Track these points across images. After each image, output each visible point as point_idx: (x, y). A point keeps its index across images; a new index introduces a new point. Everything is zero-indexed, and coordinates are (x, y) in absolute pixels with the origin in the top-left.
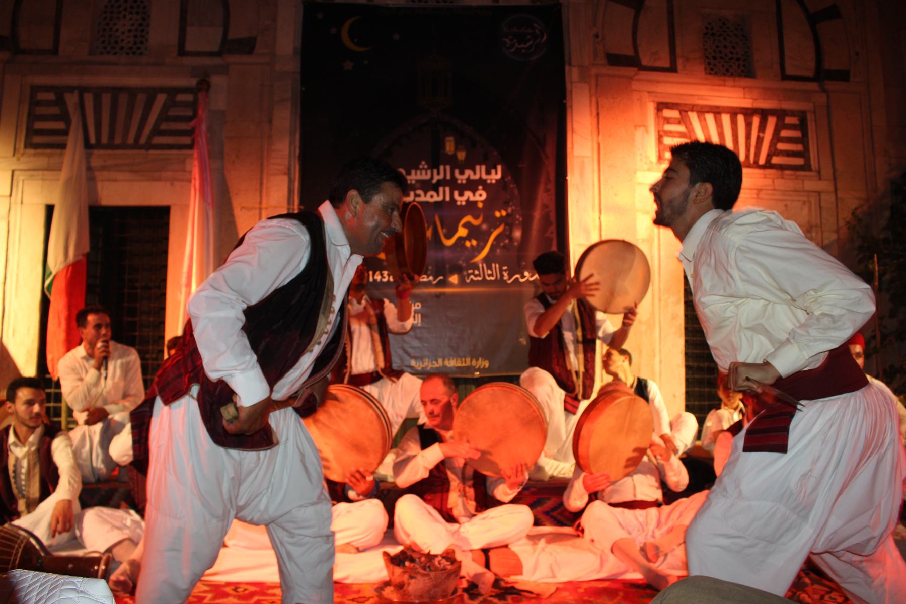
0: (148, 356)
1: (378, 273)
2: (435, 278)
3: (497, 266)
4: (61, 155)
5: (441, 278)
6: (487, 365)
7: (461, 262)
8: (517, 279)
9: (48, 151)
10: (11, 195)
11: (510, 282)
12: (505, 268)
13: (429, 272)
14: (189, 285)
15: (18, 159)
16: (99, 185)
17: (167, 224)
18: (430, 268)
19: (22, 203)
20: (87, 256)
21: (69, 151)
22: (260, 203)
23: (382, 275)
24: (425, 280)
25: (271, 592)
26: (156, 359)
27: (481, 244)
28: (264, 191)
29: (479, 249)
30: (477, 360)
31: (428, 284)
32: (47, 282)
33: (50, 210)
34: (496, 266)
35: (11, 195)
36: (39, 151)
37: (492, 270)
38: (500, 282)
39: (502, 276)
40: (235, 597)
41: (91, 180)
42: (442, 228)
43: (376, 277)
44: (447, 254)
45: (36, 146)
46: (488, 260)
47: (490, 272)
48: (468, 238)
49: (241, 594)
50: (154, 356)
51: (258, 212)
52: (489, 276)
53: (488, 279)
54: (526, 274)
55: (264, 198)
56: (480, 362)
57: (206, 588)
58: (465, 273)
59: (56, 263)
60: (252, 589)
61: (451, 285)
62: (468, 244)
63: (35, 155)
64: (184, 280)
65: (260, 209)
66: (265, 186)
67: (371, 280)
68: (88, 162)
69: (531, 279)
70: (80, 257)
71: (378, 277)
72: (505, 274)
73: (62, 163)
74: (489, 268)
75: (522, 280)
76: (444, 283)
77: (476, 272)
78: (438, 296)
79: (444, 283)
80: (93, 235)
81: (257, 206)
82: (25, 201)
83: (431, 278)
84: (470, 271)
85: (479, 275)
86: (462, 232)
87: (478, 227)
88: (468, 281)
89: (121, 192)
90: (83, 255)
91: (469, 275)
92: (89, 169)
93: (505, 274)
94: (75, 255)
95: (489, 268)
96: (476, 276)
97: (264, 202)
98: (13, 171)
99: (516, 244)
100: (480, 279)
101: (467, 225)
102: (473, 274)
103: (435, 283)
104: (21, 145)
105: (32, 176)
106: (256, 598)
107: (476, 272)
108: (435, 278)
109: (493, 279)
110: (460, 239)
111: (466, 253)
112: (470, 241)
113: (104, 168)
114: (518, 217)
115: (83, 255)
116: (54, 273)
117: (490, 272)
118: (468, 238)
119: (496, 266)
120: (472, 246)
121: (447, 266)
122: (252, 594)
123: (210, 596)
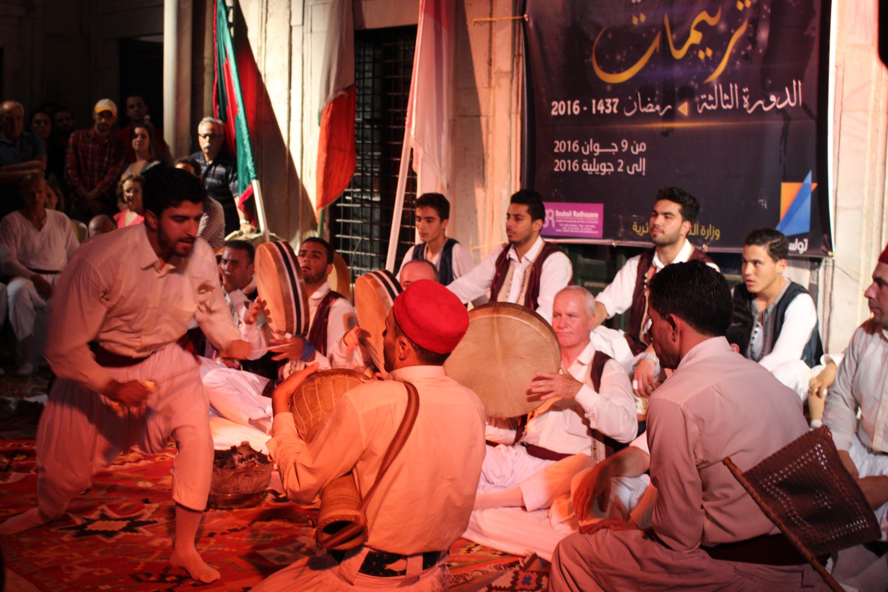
1: (601, 101)
2: (662, 108)
3: (736, 87)
5: (669, 107)
6: (718, 236)
7: (693, 83)
8: (760, 106)
10: (303, 24)
11: (750, 112)
12: (745, 90)
13: (656, 99)
18: (657, 92)
19: (311, 31)
23: (605, 104)
24: (651, 110)
27: (718, 54)
29: (714, 62)
30: (707, 228)
31: (654, 116)
34: (734, 87)
35: (303, 24)
37: (729, 95)
38: (739, 111)
39: (741, 102)
42: (672, 33)
43: (599, 108)
44: (677, 72)
46: (725, 79)
47: (726, 97)
48: (702, 46)
51: (487, 26)
52: (726, 102)
53: (724, 107)
54: (773, 98)
56: (709, 232)
58: (697, 99)
61: (681, 118)
62: (701, 55)
67: (594, 111)
69: (779, 107)
70: (340, 93)
71: (601, 108)
72: (746, 100)
74: (726, 91)
75: (766, 109)
76: (672, 115)
77: (711, 98)
78: (666, 133)
79: (672, 115)
82: (313, 30)
83: (658, 108)
84: (703, 97)
85: (713, 102)
86: (695, 37)
87: (715, 28)
88: (700, 111)
91: (702, 102)
93: (746, 100)
94: (336, 91)
95: (726, 91)
96: (709, 103)
99: (761, 51)
100: (714, 107)
101: (702, 27)
102: (706, 100)
103: (661, 114)
107: (711, 98)
108: (662, 108)
109: (730, 107)
110: (693, 47)
111: (699, 69)
112: (704, 51)
114: (765, 7)
117: (726, 97)
118: (702, 46)
119: (734, 87)
120: (706, 57)
121: (676, 90)
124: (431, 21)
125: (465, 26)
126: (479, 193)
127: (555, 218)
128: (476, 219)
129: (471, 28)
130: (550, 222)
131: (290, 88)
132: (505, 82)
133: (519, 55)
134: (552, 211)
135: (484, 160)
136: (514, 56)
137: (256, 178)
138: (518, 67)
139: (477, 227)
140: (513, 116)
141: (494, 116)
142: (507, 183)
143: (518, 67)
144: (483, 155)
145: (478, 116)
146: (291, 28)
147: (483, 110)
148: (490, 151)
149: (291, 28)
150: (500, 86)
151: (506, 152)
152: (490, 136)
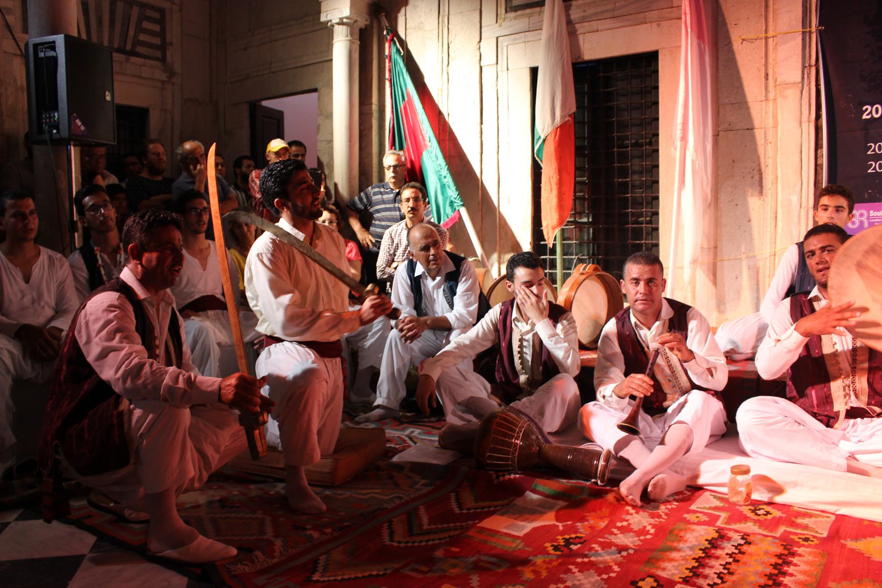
0: (641, 219)
4: (540, 13)
9: (528, 11)
14: (684, 138)
15: (500, 26)
16: (581, 38)
17: (656, 72)
20: (574, 116)
21: (547, 8)
22: (766, 31)
25: (800, 521)
26: (650, 222)
28: (771, 15)
32: (536, 148)
33: (534, 71)
36: (519, 13)
40: (756, 522)
41: (572, 34)
45: (516, 9)
49: (762, 518)
50: (648, 219)
55: (771, 23)
57: (719, 504)
59: (544, 126)
60: (776, 513)
63: (515, 18)
64: (679, 133)
65: (766, 38)
66: (771, 9)
68: (568, 16)
73: (542, 21)
80: (579, 94)
81: (763, 35)
89: (602, 43)
90: (570, 115)
92: (569, 22)
94: (562, 117)
97: (771, 28)
98: (497, 38)
104: (502, 10)
105: (515, 40)
106: (782, 529)
113: (584, 20)
115: (570, 115)
116: (543, 137)
122: (777, 522)
123: (724, 515)
124: (695, 41)
125: (729, 44)
126: (754, 202)
127: (868, 218)
128: (751, 229)
129: (737, 46)
130: (862, 223)
131: (482, 123)
132: (793, 94)
133: (810, 66)
134: (865, 212)
135: (760, 170)
136: (804, 67)
137: (463, 205)
138: (809, 77)
139: (751, 235)
140: (805, 126)
141: (775, 127)
142: (798, 189)
143: (809, 77)
144: (759, 165)
145: (752, 129)
146: (481, 68)
147: (757, 123)
148: (770, 161)
149: (481, 68)
150: (785, 98)
151: (798, 160)
152: (770, 148)
